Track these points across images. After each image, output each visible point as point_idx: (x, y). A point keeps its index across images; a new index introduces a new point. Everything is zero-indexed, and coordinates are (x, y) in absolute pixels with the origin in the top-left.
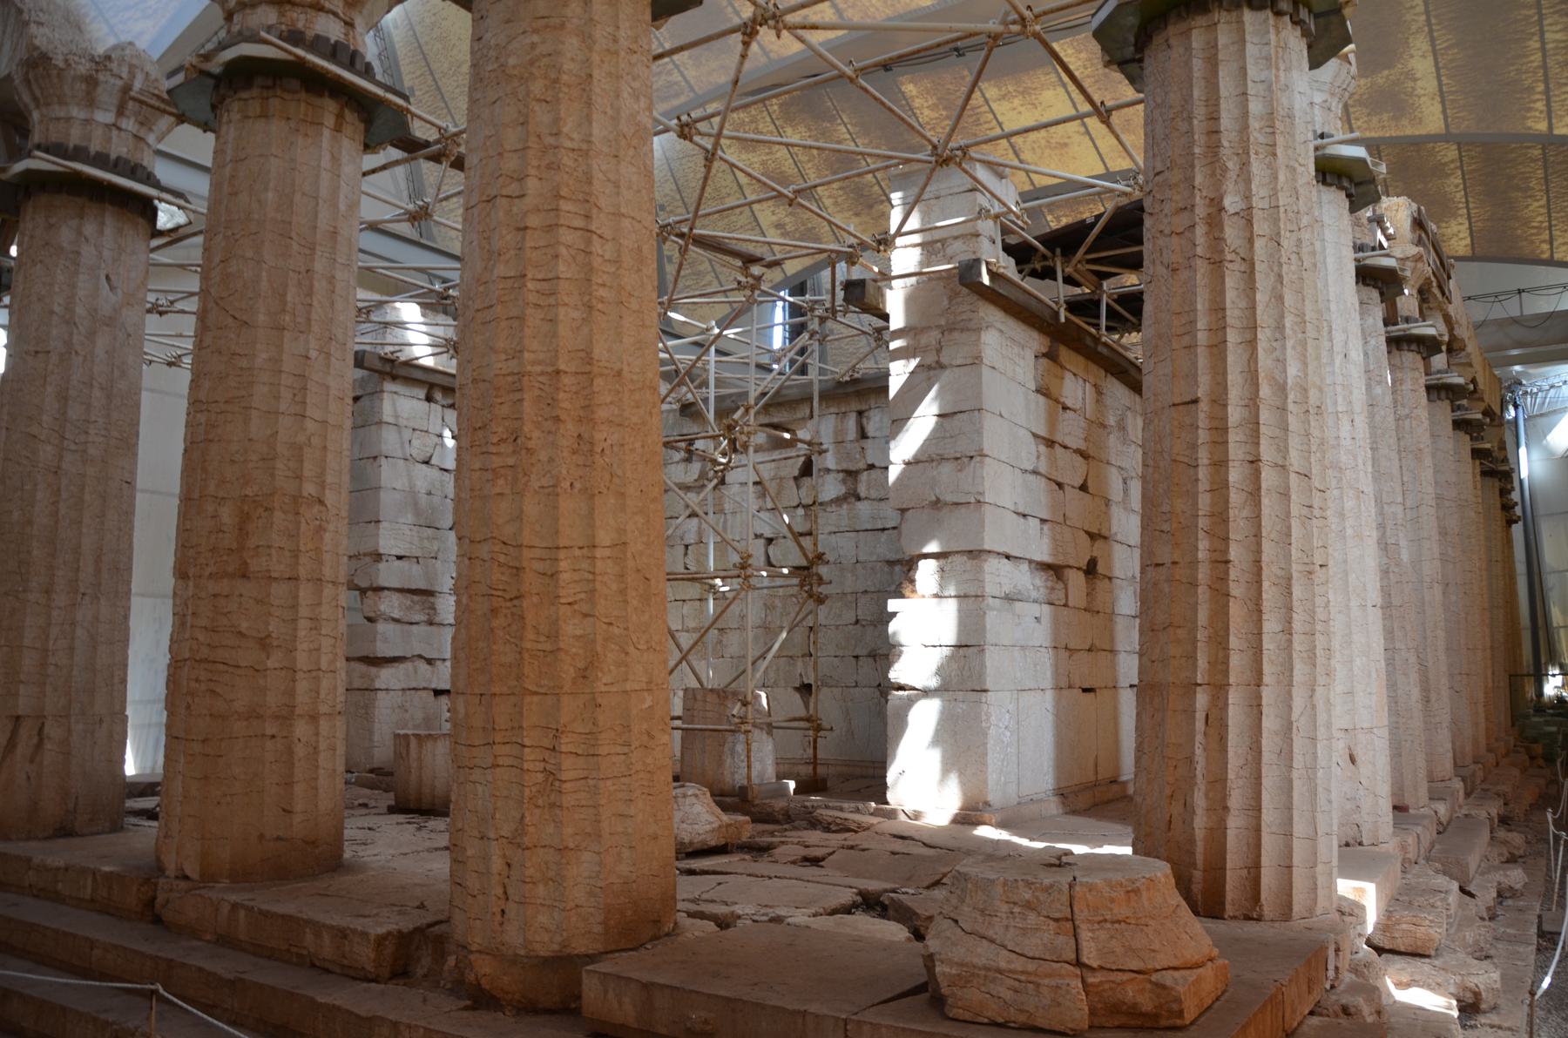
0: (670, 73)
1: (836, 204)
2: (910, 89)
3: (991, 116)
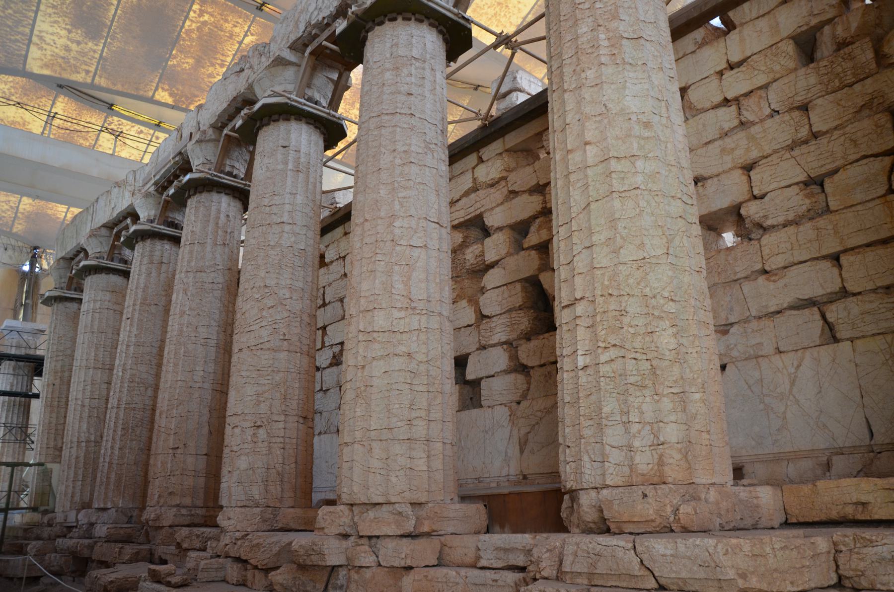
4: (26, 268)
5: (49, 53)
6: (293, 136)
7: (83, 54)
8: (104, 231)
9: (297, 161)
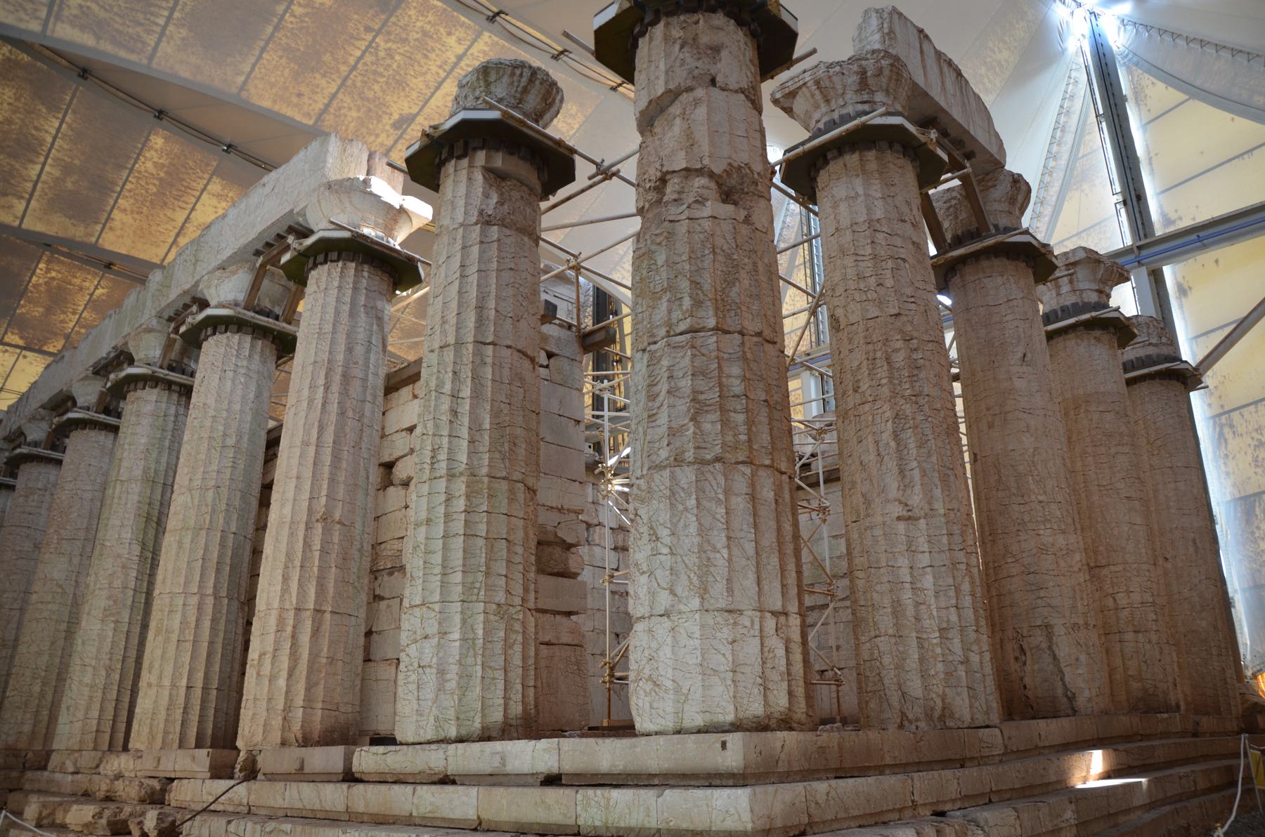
0: (149, 32)
2: (158, 141)
3: (194, 200)
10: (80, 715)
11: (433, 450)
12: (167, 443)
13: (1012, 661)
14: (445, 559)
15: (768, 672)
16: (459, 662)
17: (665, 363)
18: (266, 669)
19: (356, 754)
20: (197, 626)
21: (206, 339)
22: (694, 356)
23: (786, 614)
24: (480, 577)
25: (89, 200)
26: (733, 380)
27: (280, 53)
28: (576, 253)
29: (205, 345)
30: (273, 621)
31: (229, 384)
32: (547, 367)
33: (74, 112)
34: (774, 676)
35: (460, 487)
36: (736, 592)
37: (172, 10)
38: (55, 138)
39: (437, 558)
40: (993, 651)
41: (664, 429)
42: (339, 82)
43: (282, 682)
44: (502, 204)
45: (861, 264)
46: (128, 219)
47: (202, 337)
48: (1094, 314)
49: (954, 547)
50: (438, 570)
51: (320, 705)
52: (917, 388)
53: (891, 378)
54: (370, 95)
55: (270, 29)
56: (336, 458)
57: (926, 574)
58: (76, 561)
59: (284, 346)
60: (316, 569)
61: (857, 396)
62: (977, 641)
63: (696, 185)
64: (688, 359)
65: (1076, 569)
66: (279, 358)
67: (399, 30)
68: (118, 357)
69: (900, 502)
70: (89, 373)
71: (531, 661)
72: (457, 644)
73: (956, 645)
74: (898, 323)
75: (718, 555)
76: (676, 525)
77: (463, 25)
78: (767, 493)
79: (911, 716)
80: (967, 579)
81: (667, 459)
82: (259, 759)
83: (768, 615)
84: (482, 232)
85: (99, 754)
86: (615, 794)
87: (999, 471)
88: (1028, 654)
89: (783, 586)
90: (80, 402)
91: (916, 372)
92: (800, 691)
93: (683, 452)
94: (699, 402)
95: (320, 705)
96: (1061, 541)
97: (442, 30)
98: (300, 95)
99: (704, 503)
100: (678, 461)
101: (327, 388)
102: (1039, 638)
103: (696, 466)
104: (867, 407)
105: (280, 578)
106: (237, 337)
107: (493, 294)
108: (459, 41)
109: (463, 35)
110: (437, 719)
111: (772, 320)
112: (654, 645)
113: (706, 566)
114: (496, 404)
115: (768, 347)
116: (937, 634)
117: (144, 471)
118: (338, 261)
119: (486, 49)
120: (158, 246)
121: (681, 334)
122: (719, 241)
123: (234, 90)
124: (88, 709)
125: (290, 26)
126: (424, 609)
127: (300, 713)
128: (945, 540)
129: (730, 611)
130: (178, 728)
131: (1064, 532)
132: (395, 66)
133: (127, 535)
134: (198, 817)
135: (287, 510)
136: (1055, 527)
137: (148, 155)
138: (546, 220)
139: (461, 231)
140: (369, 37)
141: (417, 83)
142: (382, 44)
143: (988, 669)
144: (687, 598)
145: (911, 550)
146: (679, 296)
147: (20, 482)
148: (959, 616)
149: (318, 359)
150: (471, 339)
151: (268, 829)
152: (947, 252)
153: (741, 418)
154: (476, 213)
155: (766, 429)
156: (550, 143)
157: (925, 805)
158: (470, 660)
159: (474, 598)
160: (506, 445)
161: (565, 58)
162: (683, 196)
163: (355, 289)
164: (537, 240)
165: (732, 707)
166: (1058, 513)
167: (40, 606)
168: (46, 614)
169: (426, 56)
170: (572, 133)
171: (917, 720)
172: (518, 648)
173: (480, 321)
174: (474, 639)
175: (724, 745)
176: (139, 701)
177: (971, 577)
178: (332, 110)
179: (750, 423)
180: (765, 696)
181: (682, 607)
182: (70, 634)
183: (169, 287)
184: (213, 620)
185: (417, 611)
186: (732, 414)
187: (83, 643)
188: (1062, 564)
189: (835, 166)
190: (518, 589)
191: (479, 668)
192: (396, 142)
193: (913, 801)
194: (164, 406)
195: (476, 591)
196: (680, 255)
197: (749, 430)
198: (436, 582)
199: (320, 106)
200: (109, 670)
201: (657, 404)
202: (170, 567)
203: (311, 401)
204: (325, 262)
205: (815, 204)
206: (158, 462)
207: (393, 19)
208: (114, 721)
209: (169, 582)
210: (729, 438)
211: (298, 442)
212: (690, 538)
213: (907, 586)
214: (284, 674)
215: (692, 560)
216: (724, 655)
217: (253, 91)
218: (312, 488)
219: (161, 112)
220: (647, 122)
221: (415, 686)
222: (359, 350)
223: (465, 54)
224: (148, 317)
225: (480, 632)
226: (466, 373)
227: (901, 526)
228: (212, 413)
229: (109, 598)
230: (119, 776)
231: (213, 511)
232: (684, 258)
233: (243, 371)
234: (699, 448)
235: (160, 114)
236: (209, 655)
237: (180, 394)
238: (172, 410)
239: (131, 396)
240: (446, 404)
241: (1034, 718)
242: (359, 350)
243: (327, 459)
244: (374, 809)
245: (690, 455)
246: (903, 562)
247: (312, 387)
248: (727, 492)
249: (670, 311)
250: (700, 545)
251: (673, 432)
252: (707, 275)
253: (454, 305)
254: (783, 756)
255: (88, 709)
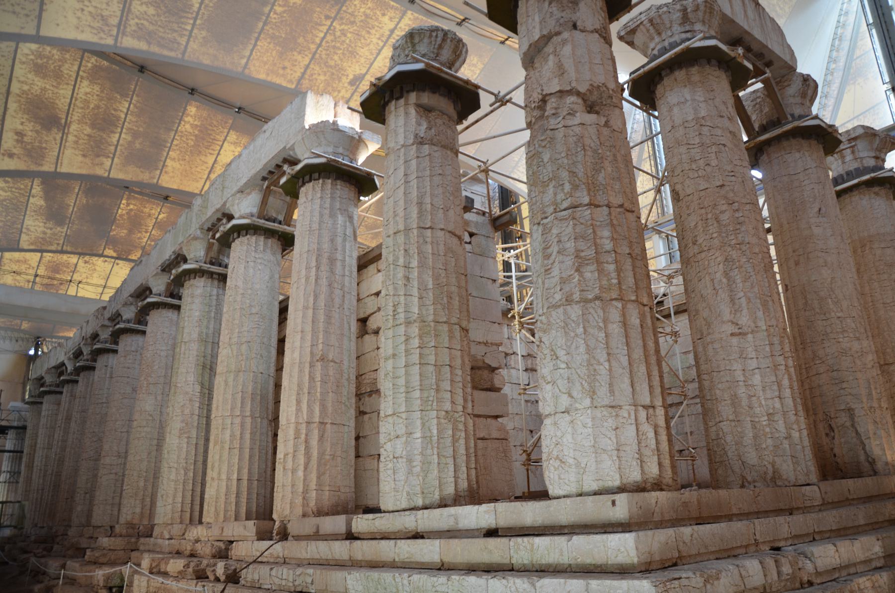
0: (181, 36)
1: (76, 142)
2: (192, 110)
3: (218, 148)
4: (32, 352)
5: (33, 236)
6: (110, 360)
7: (55, 234)
8: (53, 370)
9: (111, 373)
10: (170, 501)
11: (394, 306)
12: (213, 315)
13: (824, 436)
14: (407, 382)
15: (643, 450)
16: (422, 454)
17: (555, 231)
18: (290, 465)
19: (354, 520)
20: (241, 438)
21: (234, 240)
22: (575, 225)
23: (653, 407)
24: (433, 393)
25: (150, 155)
26: (604, 240)
27: (269, 40)
28: (485, 160)
29: (233, 245)
30: (291, 432)
31: (251, 271)
32: (470, 243)
33: (137, 96)
34: (647, 452)
35: (415, 330)
36: (616, 393)
37: (195, 19)
38: (126, 114)
39: (402, 381)
40: (809, 429)
41: (557, 279)
42: (310, 56)
43: (300, 473)
44: (430, 129)
45: (692, 150)
46: (176, 165)
47: (231, 239)
48: (873, 175)
49: (776, 353)
50: (403, 389)
51: (327, 488)
52: (740, 238)
53: (720, 233)
54: (332, 63)
55: (260, 25)
56: (329, 317)
57: (754, 374)
58: (159, 398)
59: (287, 242)
60: (318, 394)
61: (696, 247)
62: (797, 422)
63: (568, 102)
64: (570, 228)
65: (869, 366)
66: (284, 250)
67: (348, 16)
68: (176, 258)
69: (733, 323)
70: (159, 270)
71: (472, 450)
72: (420, 440)
73: (781, 425)
74: (723, 192)
75: (601, 367)
76: (570, 347)
77: (392, 7)
78: (635, 321)
79: (749, 479)
80: (786, 376)
81: (560, 300)
82: (289, 526)
83: (641, 408)
84: (418, 150)
85: (184, 526)
86: (537, 540)
87: (805, 298)
88: (836, 431)
89: (651, 387)
90: (154, 290)
91: (738, 227)
92: (667, 462)
93: (572, 295)
94: (581, 258)
95: (327, 488)
96: (856, 346)
97: (378, 12)
98: (284, 68)
99: (590, 330)
100: (569, 301)
101: (318, 268)
102: (843, 419)
103: (582, 304)
104: (703, 255)
105: (295, 402)
106: (254, 238)
107: (428, 194)
108: (391, 19)
109: (393, 15)
110: (408, 494)
111: (630, 195)
112: (559, 434)
113: (593, 376)
114: (436, 271)
115: (629, 215)
116: (766, 418)
117: (199, 335)
118: (319, 179)
119: (410, 22)
120: (197, 181)
121: (565, 210)
122: (587, 141)
123: (240, 70)
124: (174, 497)
125: (274, 21)
126: (395, 417)
127: (314, 494)
128: (768, 348)
129: (612, 407)
130: (233, 508)
131: (858, 339)
132: (347, 41)
133: (191, 378)
134: (251, 566)
135: (297, 355)
136: (851, 335)
137: (186, 119)
138: (462, 139)
139: (403, 150)
140: (328, 23)
141: (364, 52)
142: (338, 27)
143: (806, 442)
144: (581, 399)
145: (743, 356)
146: (561, 183)
147: (121, 347)
148: (782, 404)
149: (311, 249)
150: (415, 226)
151: (298, 573)
152: (755, 138)
153: (612, 267)
154: (412, 137)
155: (631, 274)
156: (460, 83)
157: (764, 542)
158: (429, 452)
159: (429, 408)
160: (445, 299)
161: (466, 24)
162: (559, 111)
163: (332, 198)
164: (457, 153)
165: (618, 476)
166: (853, 325)
167: (139, 429)
168: (143, 434)
169: (369, 32)
170: (475, 77)
171: (754, 481)
172: (462, 441)
173: (421, 213)
174: (431, 437)
175: (614, 503)
176: (207, 490)
177: (789, 375)
178: (306, 76)
179: (619, 271)
180: (642, 467)
181: (578, 405)
182: (159, 447)
183: (206, 208)
184: (251, 433)
185: (390, 419)
186: (605, 265)
187: (168, 453)
188: (858, 363)
189: (666, 81)
190: (460, 400)
191: (436, 457)
192: (352, 95)
193: (755, 540)
194: (209, 289)
195: (430, 403)
196: (560, 153)
197: (619, 275)
198: (402, 397)
199: (299, 74)
200: (186, 470)
201: (550, 261)
202: (221, 399)
203: (307, 278)
204: (310, 181)
205: (656, 110)
206: (208, 328)
207: (344, 8)
208: (192, 504)
209: (220, 408)
210: (605, 282)
211: (300, 307)
212: (580, 356)
213: (741, 383)
214: (302, 468)
215: (583, 371)
216: (610, 439)
217: (252, 69)
218: (312, 338)
219: (193, 90)
220: (530, 60)
221: (392, 471)
222: (339, 240)
223: (395, 28)
224: (194, 229)
225: (435, 432)
226: (413, 250)
227: (735, 341)
228: (241, 291)
229: (182, 422)
230: (197, 541)
231: (247, 359)
232: (563, 155)
233: (259, 261)
234: (583, 290)
235: (192, 91)
236: (251, 457)
237: (219, 281)
238: (215, 292)
239: (187, 284)
240: (401, 273)
241: (843, 478)
242: (339, 240)
243: (322, 317)
244: (369, 557)
245: (576, 297)
246: (737, 366)
247: (308, 268)
248: (605, 321)
249: (555, 194)
250: (588, 360)
251: (563, 281)
252: (580, 166)
253: (402, 203)
254: (657, 509)
255: (174, 497)
